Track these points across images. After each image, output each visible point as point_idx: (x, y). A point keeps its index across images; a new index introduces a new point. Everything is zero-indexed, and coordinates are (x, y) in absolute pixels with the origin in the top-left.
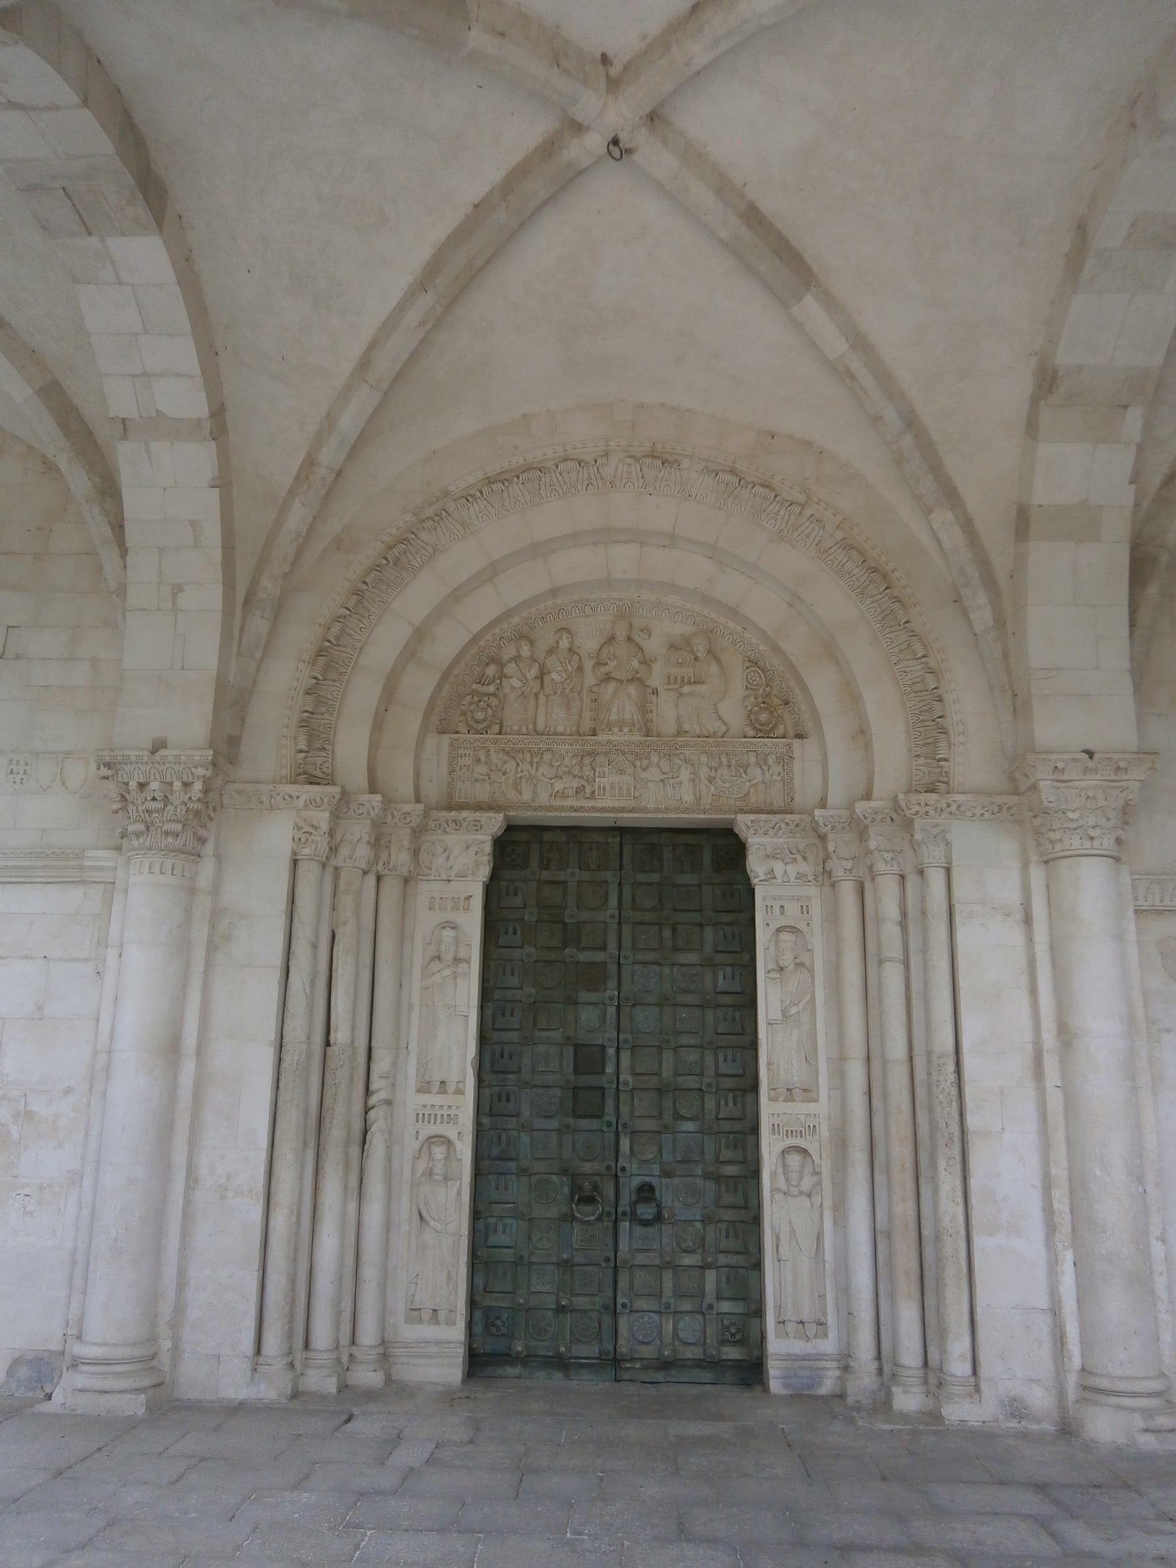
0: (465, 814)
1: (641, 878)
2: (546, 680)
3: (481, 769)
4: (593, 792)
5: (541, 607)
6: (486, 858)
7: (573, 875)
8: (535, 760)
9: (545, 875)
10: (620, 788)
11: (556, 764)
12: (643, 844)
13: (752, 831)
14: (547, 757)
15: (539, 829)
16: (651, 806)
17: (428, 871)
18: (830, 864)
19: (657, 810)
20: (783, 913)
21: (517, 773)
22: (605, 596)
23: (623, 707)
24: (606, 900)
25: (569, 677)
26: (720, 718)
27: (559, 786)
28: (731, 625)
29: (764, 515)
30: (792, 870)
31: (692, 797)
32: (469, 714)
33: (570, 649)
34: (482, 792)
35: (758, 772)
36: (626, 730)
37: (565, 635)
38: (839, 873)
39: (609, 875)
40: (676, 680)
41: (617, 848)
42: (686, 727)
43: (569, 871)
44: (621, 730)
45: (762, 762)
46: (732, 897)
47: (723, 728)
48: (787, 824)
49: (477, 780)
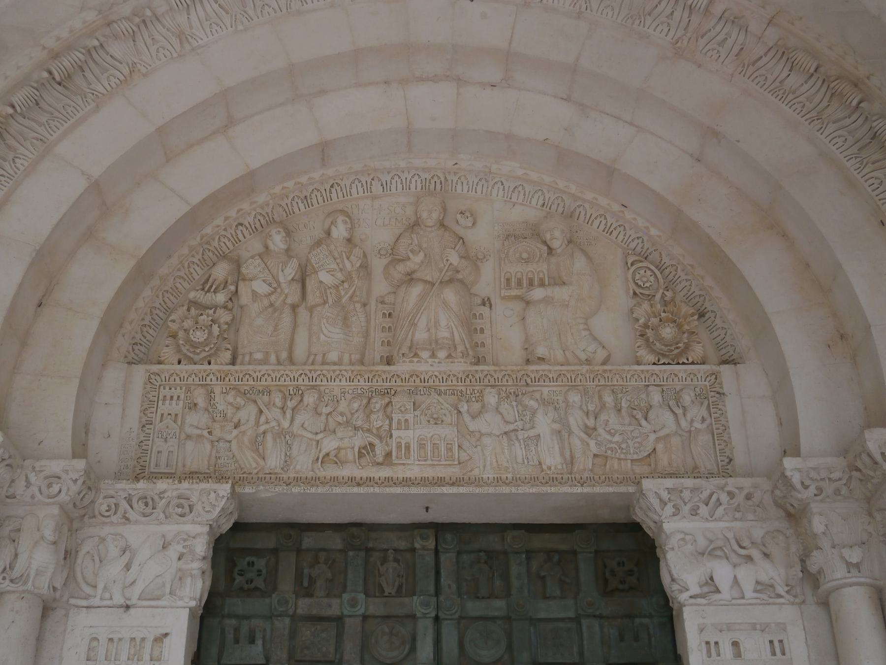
0: (161, 485)
1: (474, 608)
2: (311, 284)
3: (196, 420)
4: (389, 455)
5: (304, 179)
6: (196, 566)
7: (352, 604)
8: (290, 404)
9: (304, 606)
10: (435, 446)
11: (326, 410)
12: (475, 553)
13: (669, 509)
14: (310, 399)
15: (293, 531)
16: (489, 474)
17: (88, 590)
18: (816, 561)
19: (498, 481)
20: (738, 655)
21: (257, 424)
22: (403, 164)
23: (437, 324)
24: (413, 649)
25: (348, 278)
26: (595, 339)
27: (329, 445)
28: (603, 201)
29: (649, 20)
30: (747, 576)
31: (559, 459)
32: (181, 334)
33: (349, 240)
34: (196, 455)
35: (668, 417)
36: (442, 354)
37: (340, 218)
38: (837, 573)
39: (415, 604)
40: (519, 283)
41: (430, 559)
42: (541, 351)
43: (346, 597)
44: (433, 356)
45: (673, 401)
46: (636, 639)
47: (601, 354)
48: (731, 494)
49: (189, 437)
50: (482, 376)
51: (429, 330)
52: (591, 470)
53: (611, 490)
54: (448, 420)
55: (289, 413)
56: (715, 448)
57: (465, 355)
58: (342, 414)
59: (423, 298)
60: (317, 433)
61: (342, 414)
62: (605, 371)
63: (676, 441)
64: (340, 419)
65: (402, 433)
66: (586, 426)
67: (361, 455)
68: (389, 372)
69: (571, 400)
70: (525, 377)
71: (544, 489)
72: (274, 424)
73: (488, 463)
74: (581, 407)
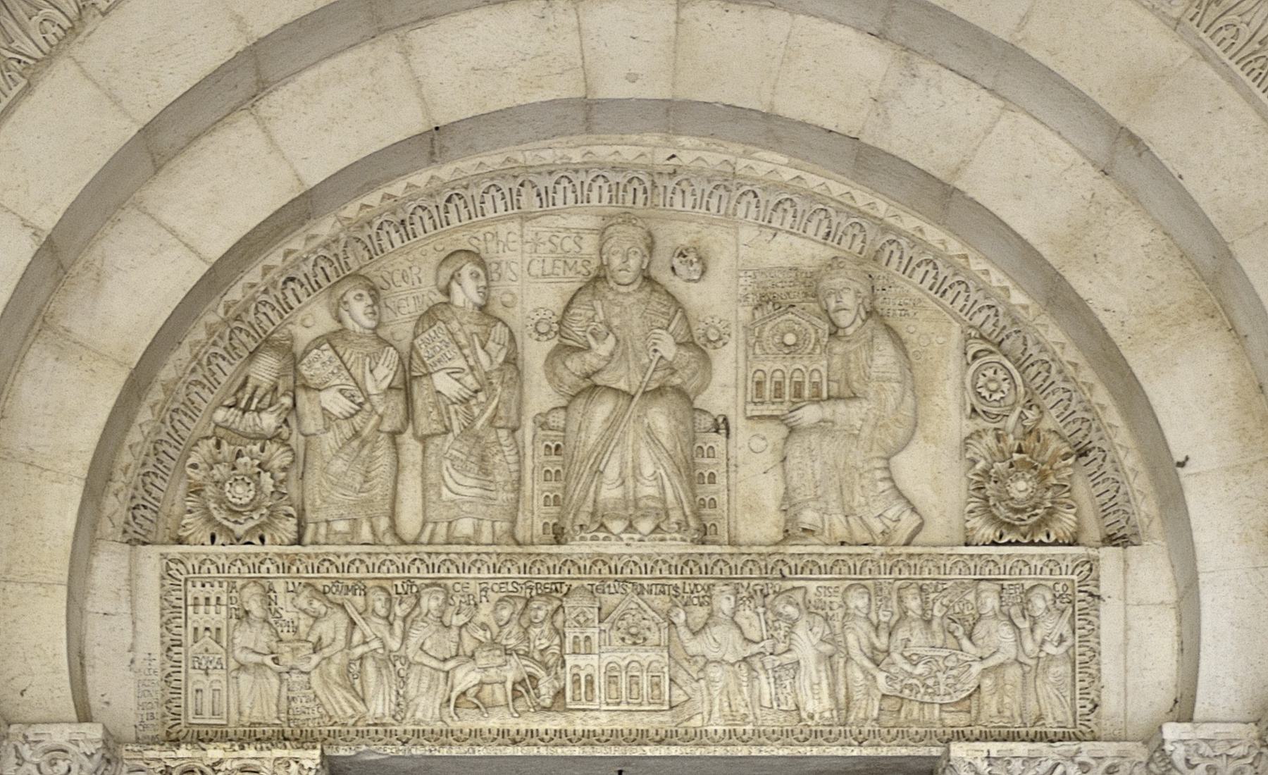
3: (251, 637)
4: (560, 693)
8: (399, 611)
11: (458, 620)
14: (430, 602)
23: (637, 469)
27: (466, 678)
31: (827, 702)
34: (256, 699)
35: (1006, 632)
36: (645, 526)
44: (631, 527)
49: (242, 667)
50: (710, 563)
51: (623, 482)
52: (877, 720)
53: (904, 751)
54: (653, 637)
55: (398, 625)
56: (1074, 686)
57: (682, 526)
58: (484, 627)
59: (613, 424)
60: (445, 660)
61: (484, 627)
62: (910, 556)
63: (1013, 673)
64: (480, 634)
65: (581, 661)
66: (874, 648)
67: (516, 695)
68: (558, 555)
69: (852, 605)
70: (780, 565)
71: (802, 750)
72: (375, 644)
73: (716, 708)
74: (868, 618)
